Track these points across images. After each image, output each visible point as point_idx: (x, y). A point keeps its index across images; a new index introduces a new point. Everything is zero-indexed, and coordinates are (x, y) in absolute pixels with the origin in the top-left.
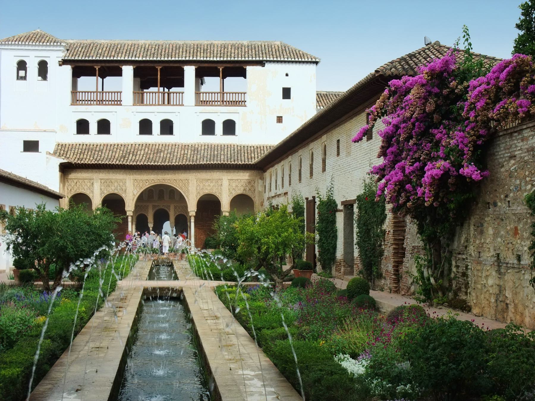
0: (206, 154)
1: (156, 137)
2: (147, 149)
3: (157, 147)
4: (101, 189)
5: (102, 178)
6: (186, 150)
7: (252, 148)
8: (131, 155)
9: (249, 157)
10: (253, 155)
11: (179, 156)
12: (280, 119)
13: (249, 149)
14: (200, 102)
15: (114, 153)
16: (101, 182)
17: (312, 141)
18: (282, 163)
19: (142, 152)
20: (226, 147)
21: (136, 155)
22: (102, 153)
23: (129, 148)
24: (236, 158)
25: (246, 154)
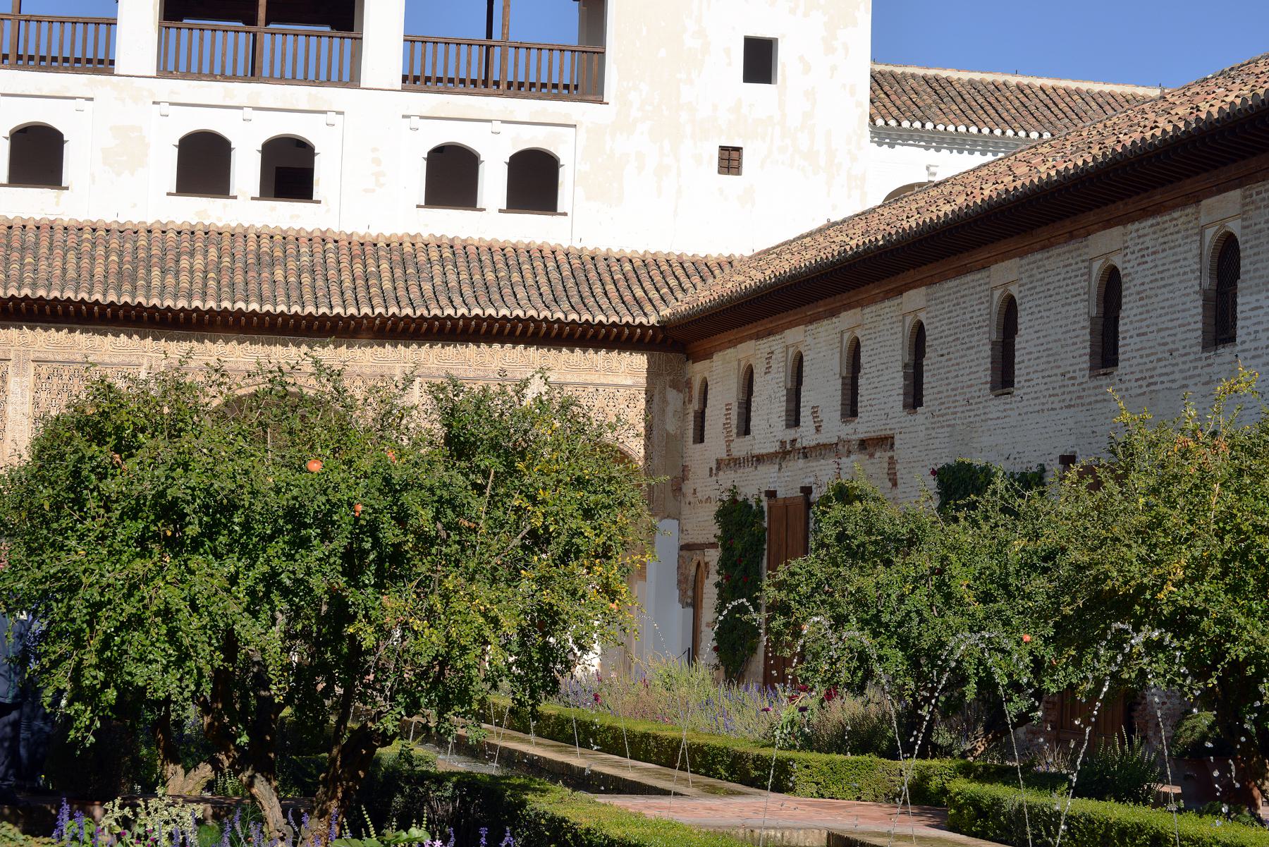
0: (452, 277)
1: (245, 207)
2: (213, 252)
3: (252, 246)
4: (36, 404)
5: (42, 356)
6: (370, 261)
7: (628, 267)
8: (156, 272)
9: (628, 297)
10: (639, 293)
11: (347, 283)
12: (730, 160)
13: (616, 268)
14: (412, 81)
15: (85, 262)
16: (38, 375)
17: (1108, 224)
18: (847, 319)
19: (199, 262)
20: (524, 258)
21: (177, 273)
22: (37, 259)
23: (143, 242)
24: (575, 299)
25: (610, 287)
